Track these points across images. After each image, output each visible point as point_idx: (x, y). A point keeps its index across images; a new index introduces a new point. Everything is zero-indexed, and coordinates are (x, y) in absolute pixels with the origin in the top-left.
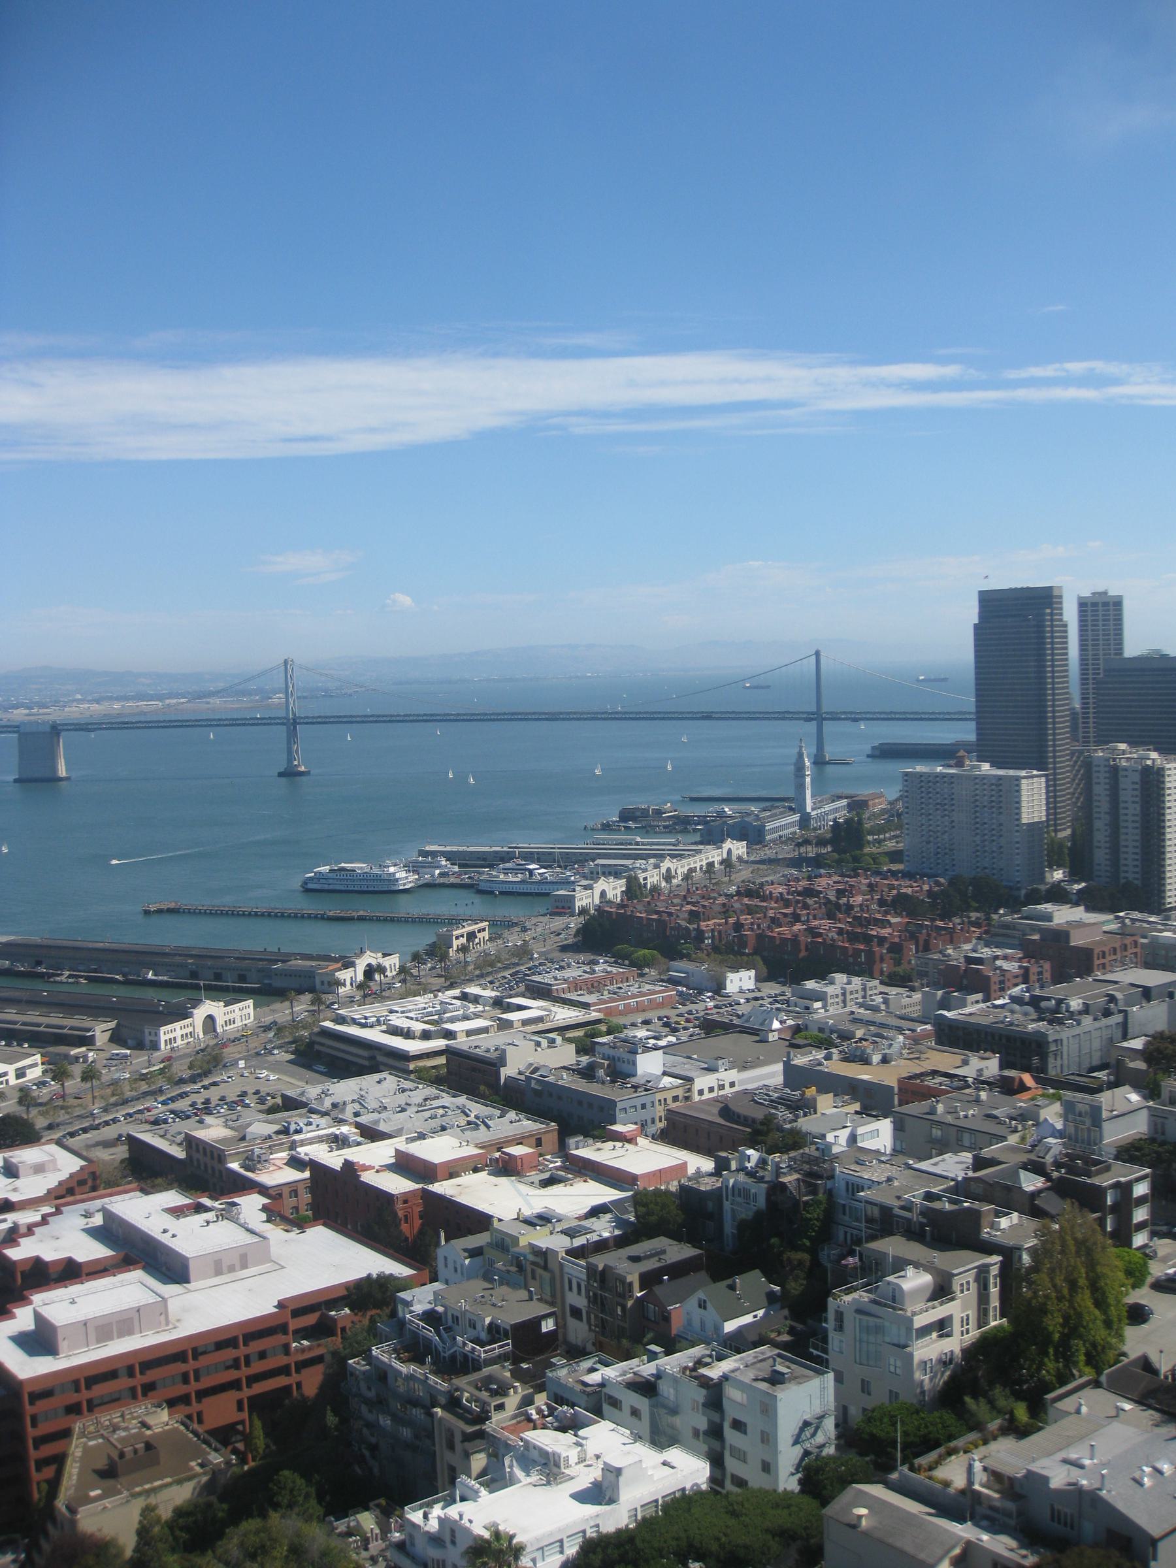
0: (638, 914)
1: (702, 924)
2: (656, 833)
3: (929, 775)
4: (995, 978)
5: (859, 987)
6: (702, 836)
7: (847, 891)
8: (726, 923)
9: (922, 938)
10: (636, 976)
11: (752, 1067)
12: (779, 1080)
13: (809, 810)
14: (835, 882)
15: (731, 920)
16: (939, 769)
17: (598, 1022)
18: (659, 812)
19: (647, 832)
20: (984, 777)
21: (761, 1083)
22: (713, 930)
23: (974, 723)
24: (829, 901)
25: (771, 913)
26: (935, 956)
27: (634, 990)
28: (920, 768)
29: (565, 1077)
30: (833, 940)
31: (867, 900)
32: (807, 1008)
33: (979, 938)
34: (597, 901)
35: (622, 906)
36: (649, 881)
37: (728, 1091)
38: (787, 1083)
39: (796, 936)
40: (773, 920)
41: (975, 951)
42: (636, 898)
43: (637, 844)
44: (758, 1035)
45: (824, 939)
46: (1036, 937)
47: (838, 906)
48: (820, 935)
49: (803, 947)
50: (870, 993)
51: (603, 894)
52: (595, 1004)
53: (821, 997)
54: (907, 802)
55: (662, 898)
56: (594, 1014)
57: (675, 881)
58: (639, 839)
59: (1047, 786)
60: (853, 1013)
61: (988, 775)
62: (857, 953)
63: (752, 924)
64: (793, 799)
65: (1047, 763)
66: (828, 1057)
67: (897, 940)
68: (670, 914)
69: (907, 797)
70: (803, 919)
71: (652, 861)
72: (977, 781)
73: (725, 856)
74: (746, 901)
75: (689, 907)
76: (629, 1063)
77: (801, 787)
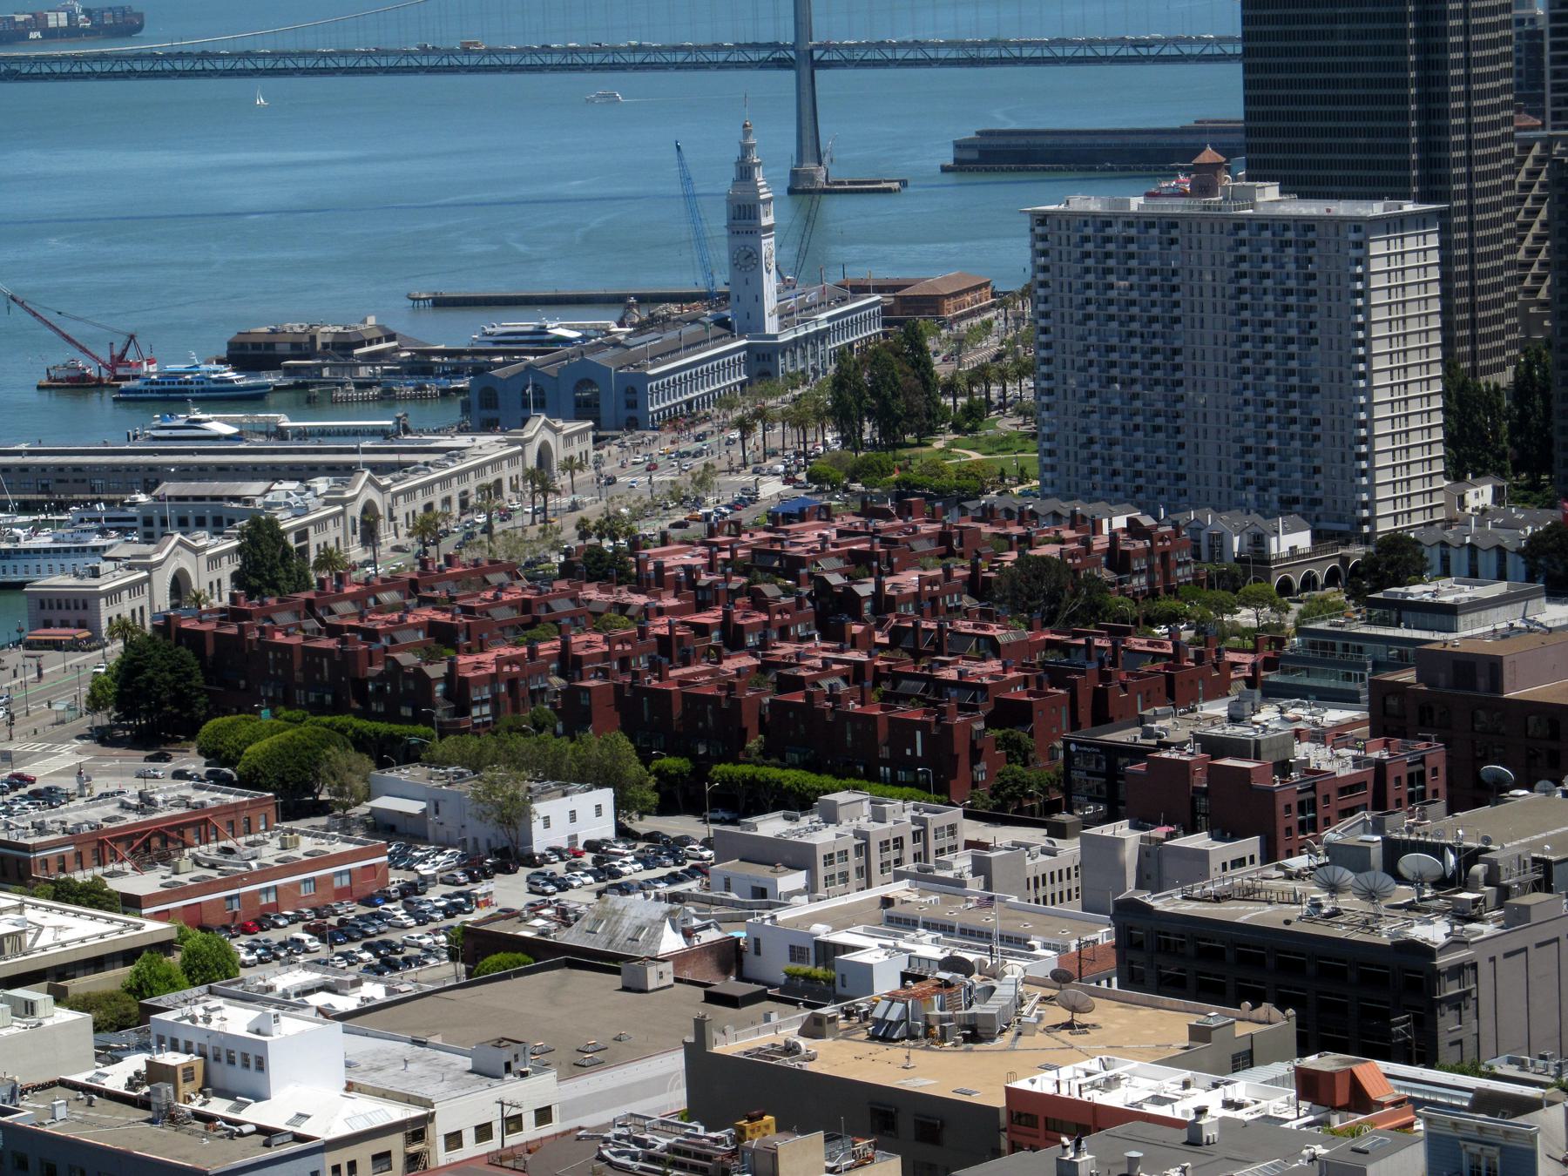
0: (279, 637)
1: (463, 660)
2: (334, 402)
3: (1105, 222)
4: (1287, 792)
5: (907, 830)
6: (466, 408)
7: (877, 556)
8: (533, 653)
9: (1087, 684)
10: (273, 816)
11: (598, 1065)
12: (677, 1098)
13: (771, 325)
14: (841, 533)
15: (547, 648)
16: (1136, 203)
17: (165, 947)
18: (343, 347)
19: (310, 400)
20: (1264, 224)
21: (620, 1111)
22: (493, 679)
23: (1235, 73)
24: (822, 585)
25: (659, 627)
26: (1126, 736)
27: (270, 853)
28: (1087, 201)
29: (61, 1112)
30: (833, 697)
31: (932, 581)
32: (760, 893)
33: (1251, 683)
34: (163, 602)
35: (232, 614)
36: (314, 540)
37: (531, 1131)
38: (694, 1111)
39: (731, 687)
40: (664, 643)
41: (1234, 719)
42: (273, 585)
43: (281, 434)
44: (617, 971)
45: (809, 696)
46: (1408, 676)
47: (848, 603)
48: (797, 683)
49: (750, 721)
50: (932, 845)
51: (179, 584)
52: (154, 899)
53: (798, 857)
54: (1048, 377)
55: (348, 590)
56: (151, 926)
57: (387, 538)
58: (285, 422)
59: (1446, 263)
60: (887, 902)
61: (1274, 219)
62: (903, 730)
63: (606, 656)
64: (726, 297)
65: (1447, 180)
66: (814, 1029)
67: (1018, 693)
68: (371, 635)
69: (1047, 361)
70: (751, 640)
71: (321, 484)
72: (1244, 234)
73: (532, 462)
74: (592, 593)
75: (426, 614)
76: (246, 1065)
77: (747, 261)
